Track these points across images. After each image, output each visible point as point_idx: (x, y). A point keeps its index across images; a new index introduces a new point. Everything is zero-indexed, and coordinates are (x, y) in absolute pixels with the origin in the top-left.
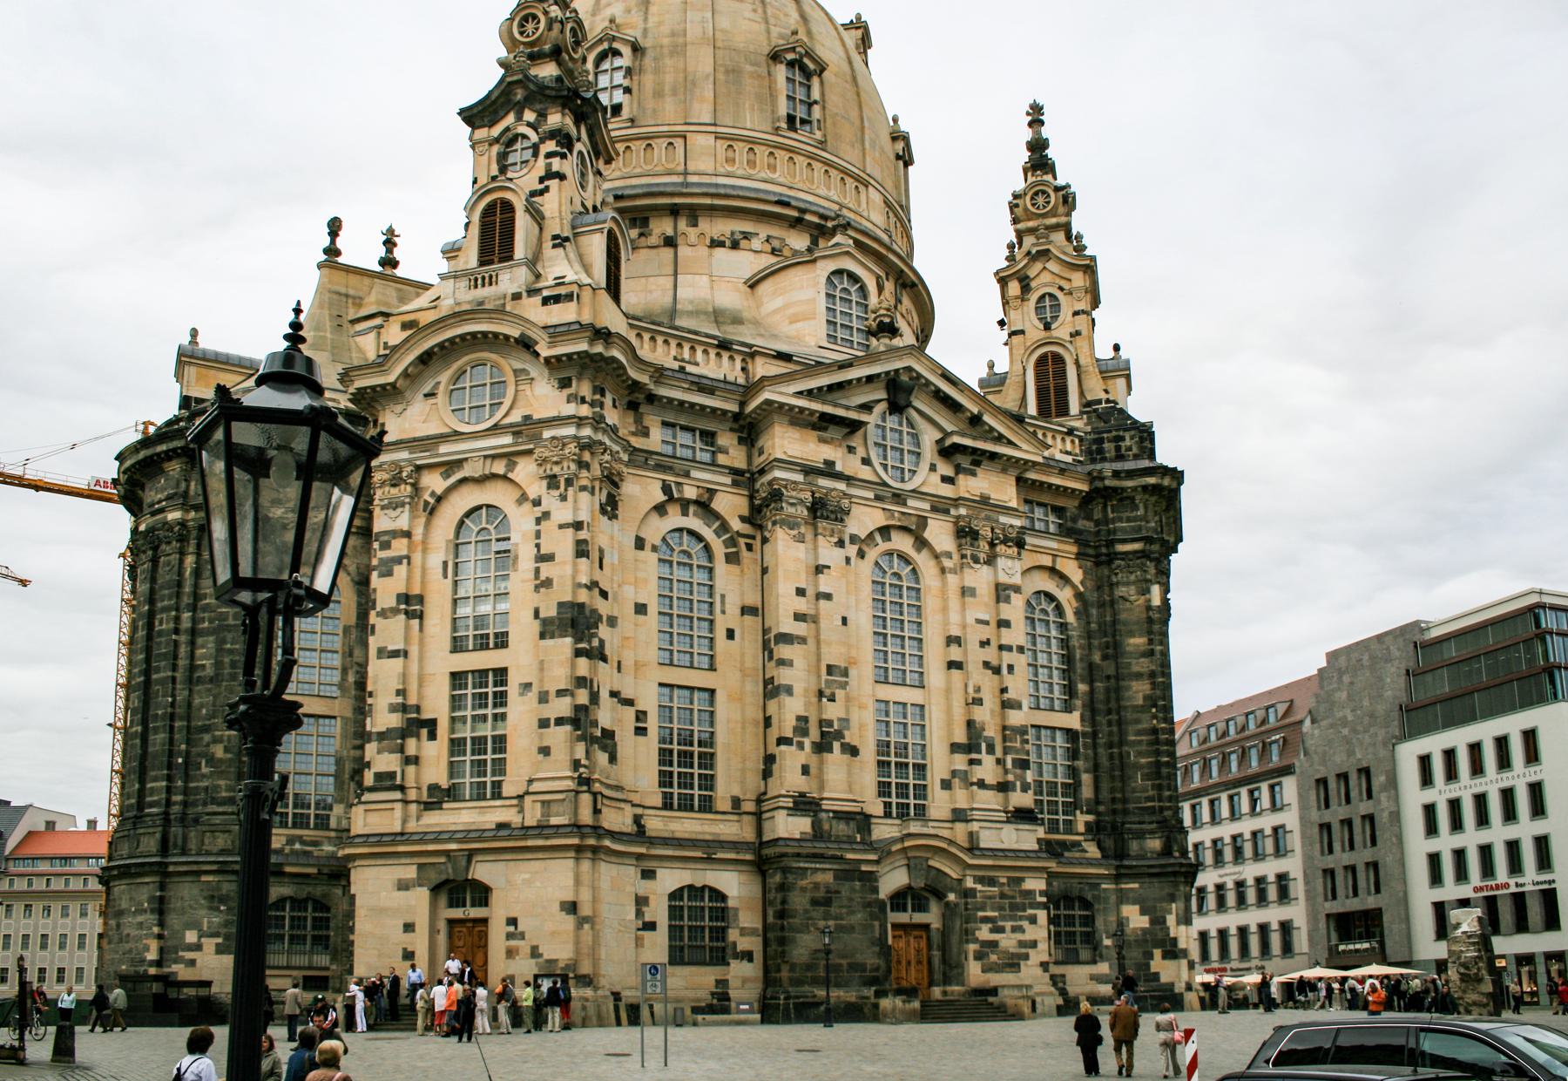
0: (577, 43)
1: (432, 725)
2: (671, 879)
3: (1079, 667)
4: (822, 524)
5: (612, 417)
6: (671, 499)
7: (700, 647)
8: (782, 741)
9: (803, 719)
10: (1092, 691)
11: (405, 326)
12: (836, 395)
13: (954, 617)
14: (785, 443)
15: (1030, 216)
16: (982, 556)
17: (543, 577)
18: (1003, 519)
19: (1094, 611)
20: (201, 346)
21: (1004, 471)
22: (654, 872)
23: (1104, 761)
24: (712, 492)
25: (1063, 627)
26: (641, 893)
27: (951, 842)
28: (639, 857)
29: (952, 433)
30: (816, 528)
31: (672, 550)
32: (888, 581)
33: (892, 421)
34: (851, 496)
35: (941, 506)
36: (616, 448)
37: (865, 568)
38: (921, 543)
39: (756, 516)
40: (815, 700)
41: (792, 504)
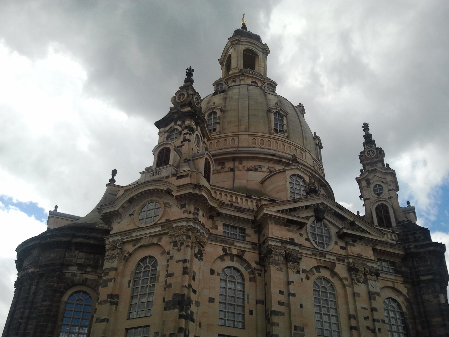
0: (198, 103)
4: (290, 264)
5: (202, 220)
6: (226, 254)
12: (294, 213)
13: (351, 306)
16: (361, 279)
18: (368, 264)
20: (58, 211)
21: (367, 244)
24: (243, 252)
25: (402, 314)
29: (342, 228)
30: (287, 266)
31: (227, 275)
32: (320, 290)
33: (317, 225)
34: (302, 253)
35: (340, 259)
36: (202, 231)
37: (309, 284)
41: (277, 255)
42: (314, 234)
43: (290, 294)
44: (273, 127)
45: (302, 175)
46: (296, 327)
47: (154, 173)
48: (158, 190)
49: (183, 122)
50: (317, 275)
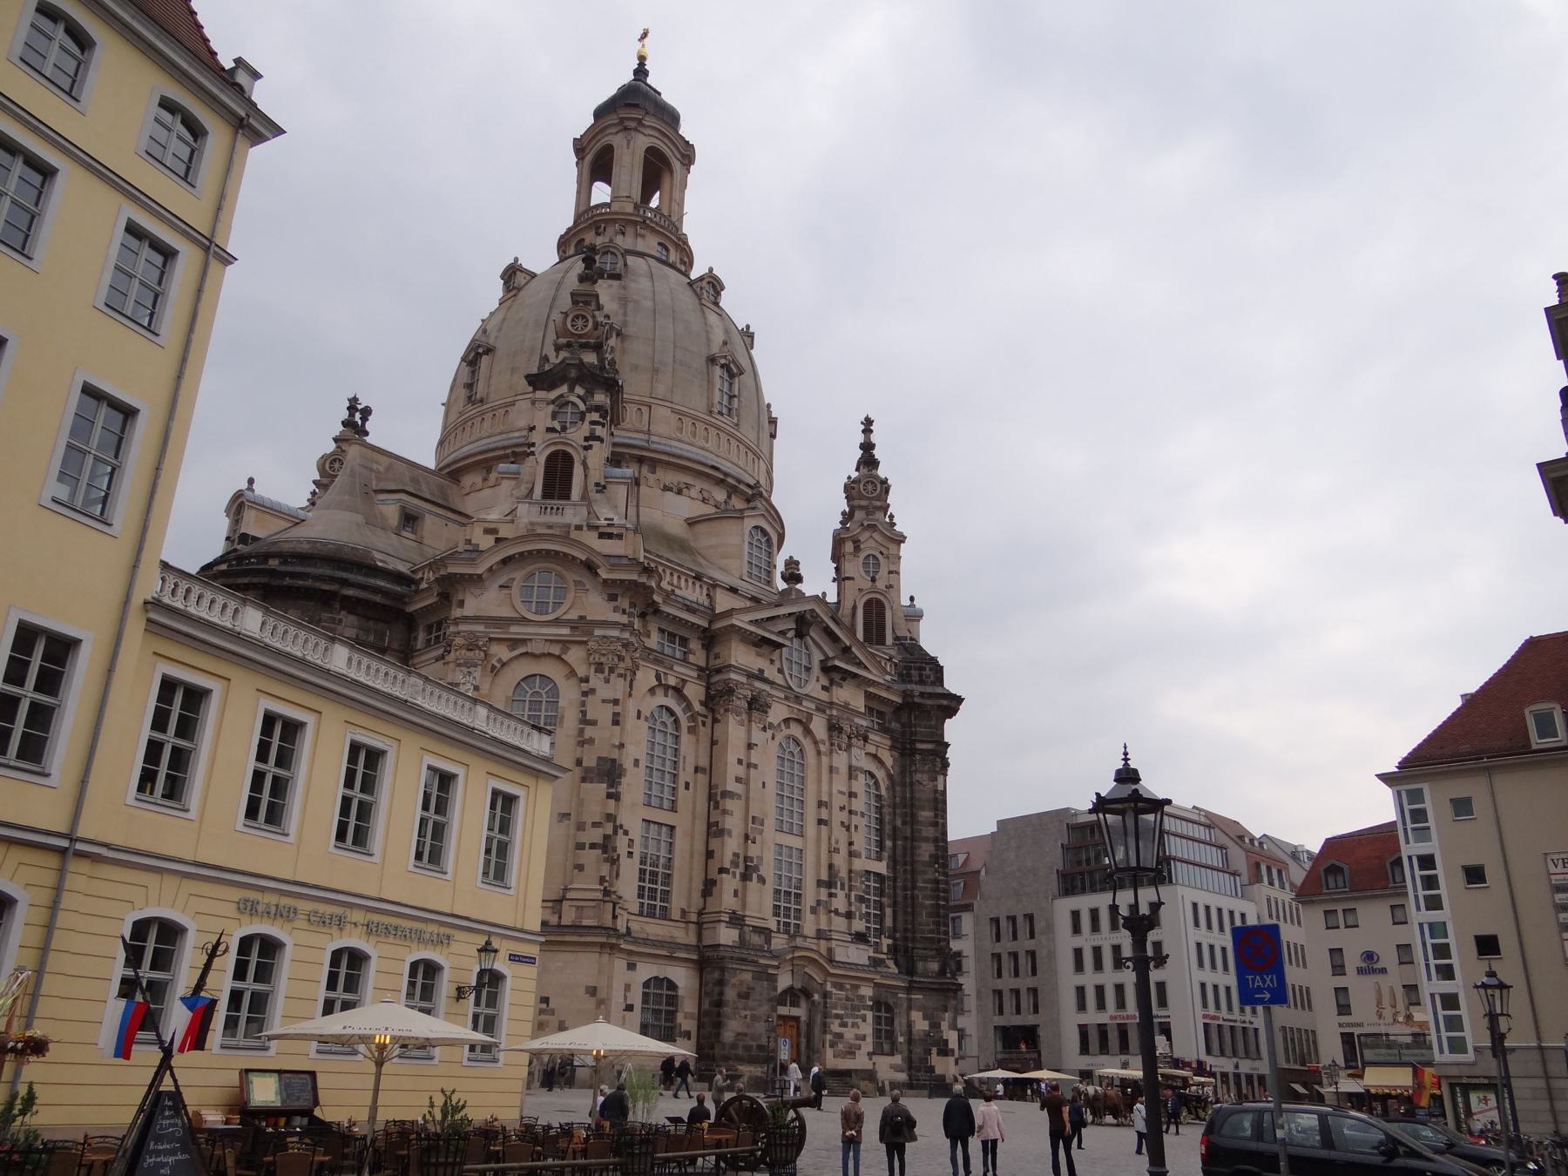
2: (646, 971)
3: (888, 828)
4: (755, 714)
5: (637, 624)
7: (667, 795)
8: (722, 870)
9: (736, 855)
11: (488, 531)
13: (825, 787)
14: (741, 656)
15: (862, 497)
18: (857, 720)
21: (858, 686)
23: (900, 899)
25: (879, 797)
27: (818, 952)
28: (630, 953)
35: (822, 707)
37: (774, 747)
39: (710, 701)
40: (742, 840)
43: (749, 765)
48: (565, 555)
49: (590, 393)
50: (786, 732)
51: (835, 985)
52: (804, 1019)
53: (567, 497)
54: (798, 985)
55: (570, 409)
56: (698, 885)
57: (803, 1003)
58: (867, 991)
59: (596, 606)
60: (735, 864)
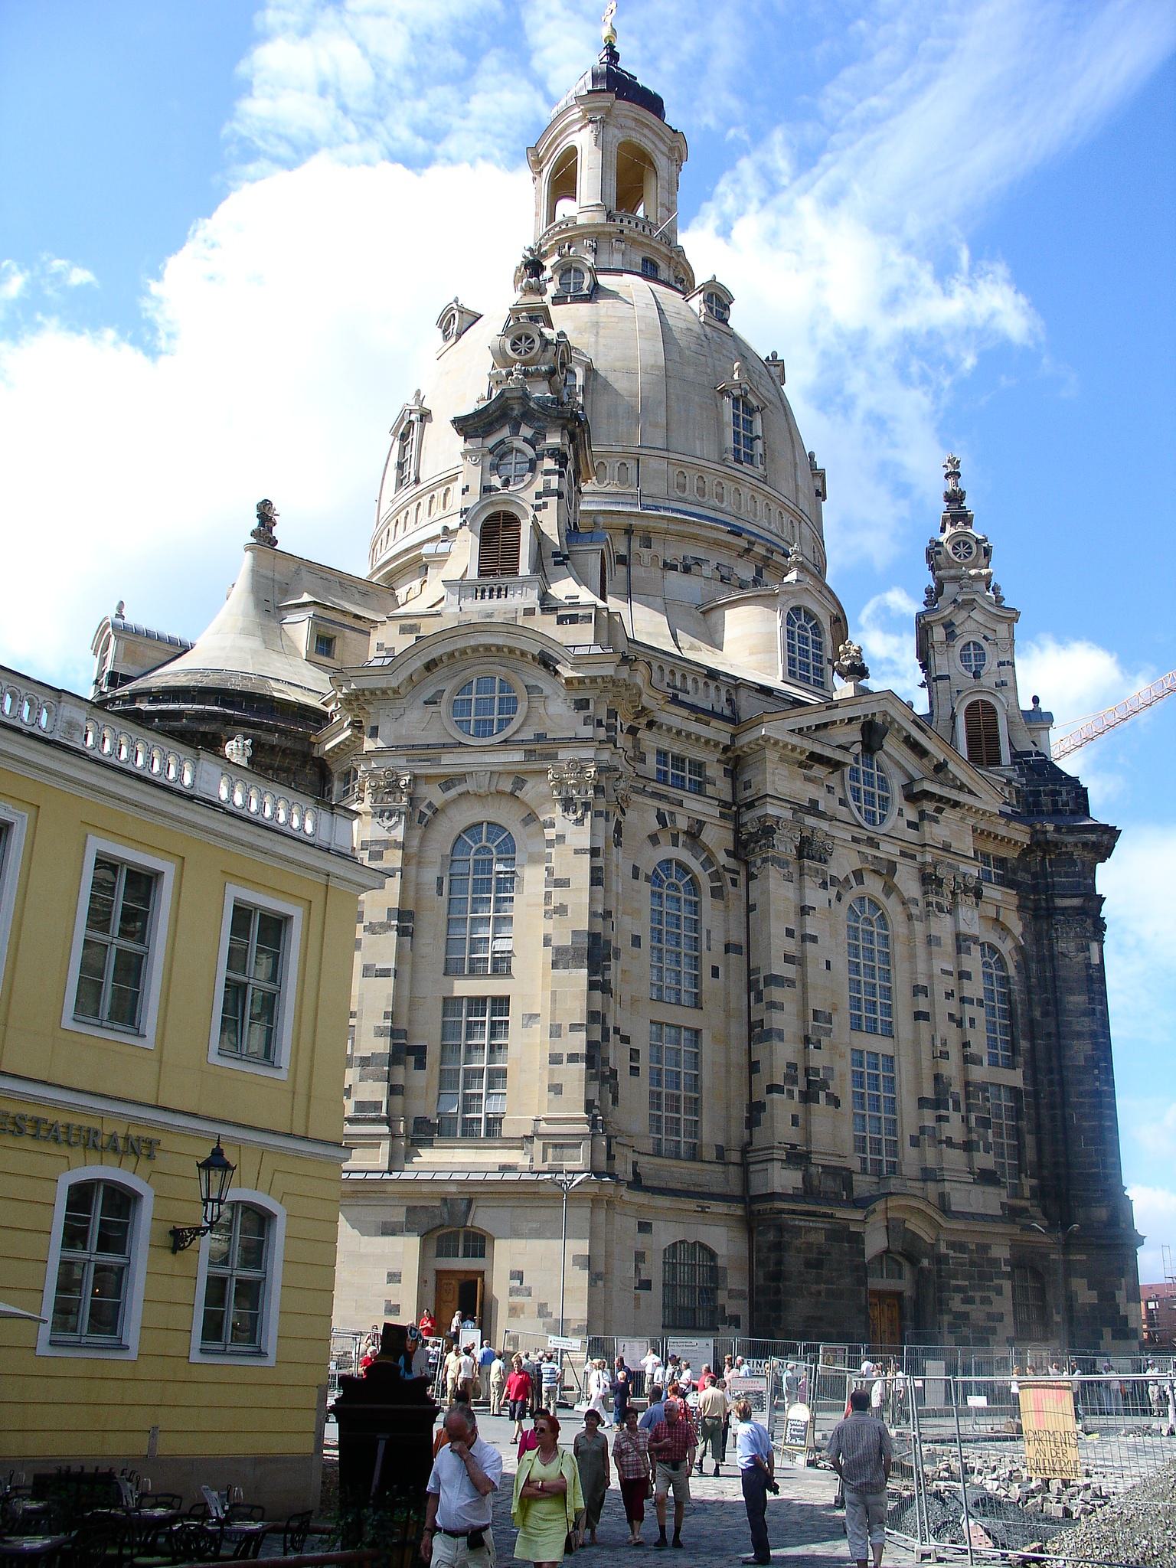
1: (420, 1053)
2: (665, 1234)
4: (807, 862)
5: (623, 740)
7: (686, 985)
8: (772, 1089)
9: (791, 1066)
10: (1033, 1049)
12: (821, 734)
16: (946, 903)
17: (556, 901)
19: (1034, 966)
22: (650, 1225)
24: (701, 824)
26: (640, 1248)
27: (925, 1199)
30: (801, 868)
37: (842, 910)
38: (890, 889)
40: (801, 1046)
42: (856, 792)
43: (805, 938)
44: (730, 443)
45: (815, 608)
46: (815, 1011)
47: (483, 591)
51: (951, 1245)
52: (908, 1293)
53: (514, 571)
54: (898, 1246)
55: (512, 458)
56: (740, 1112)
57: (907, 1269)
58: (1001, 1252)
59: (558, 714)
60: (791, 1079)
